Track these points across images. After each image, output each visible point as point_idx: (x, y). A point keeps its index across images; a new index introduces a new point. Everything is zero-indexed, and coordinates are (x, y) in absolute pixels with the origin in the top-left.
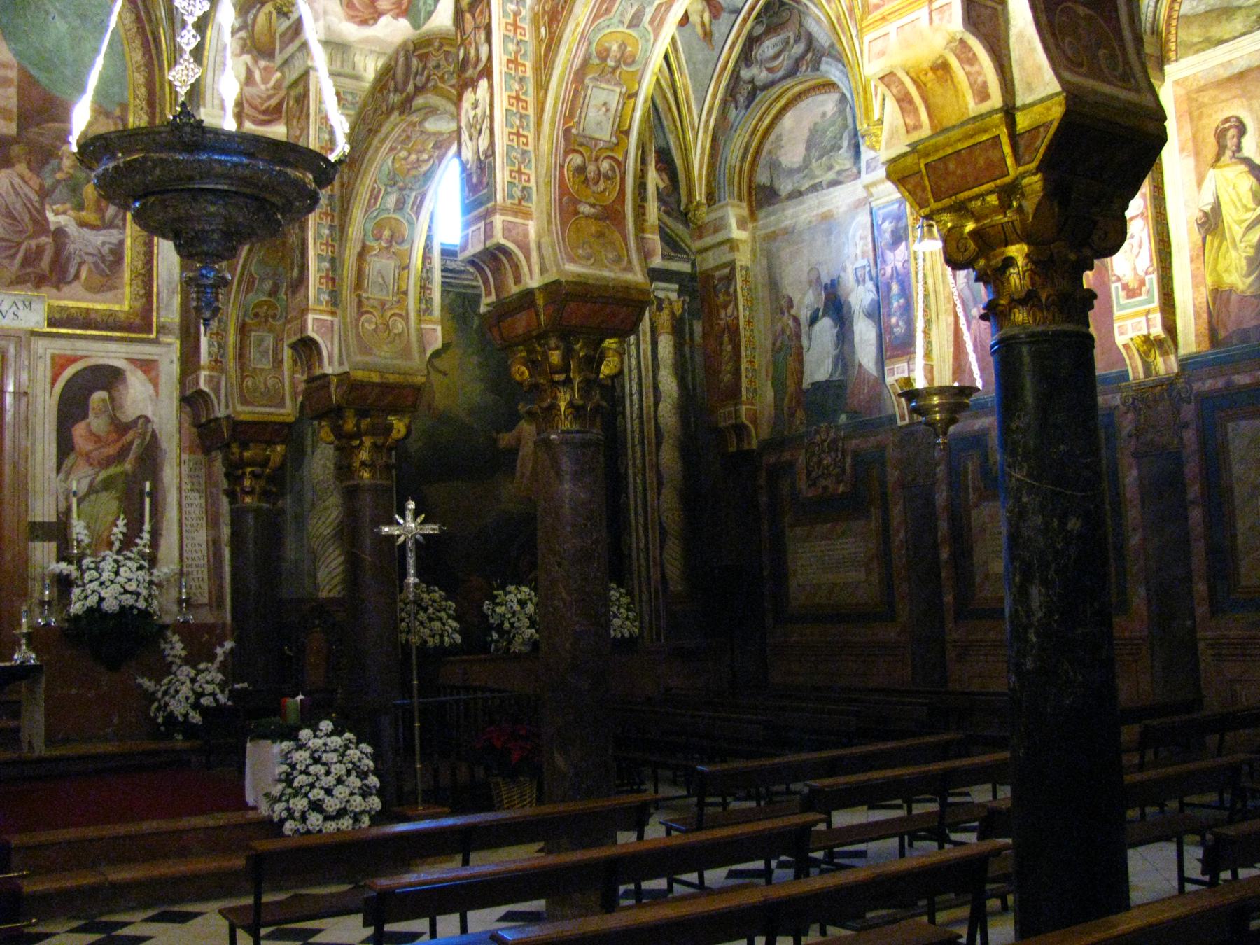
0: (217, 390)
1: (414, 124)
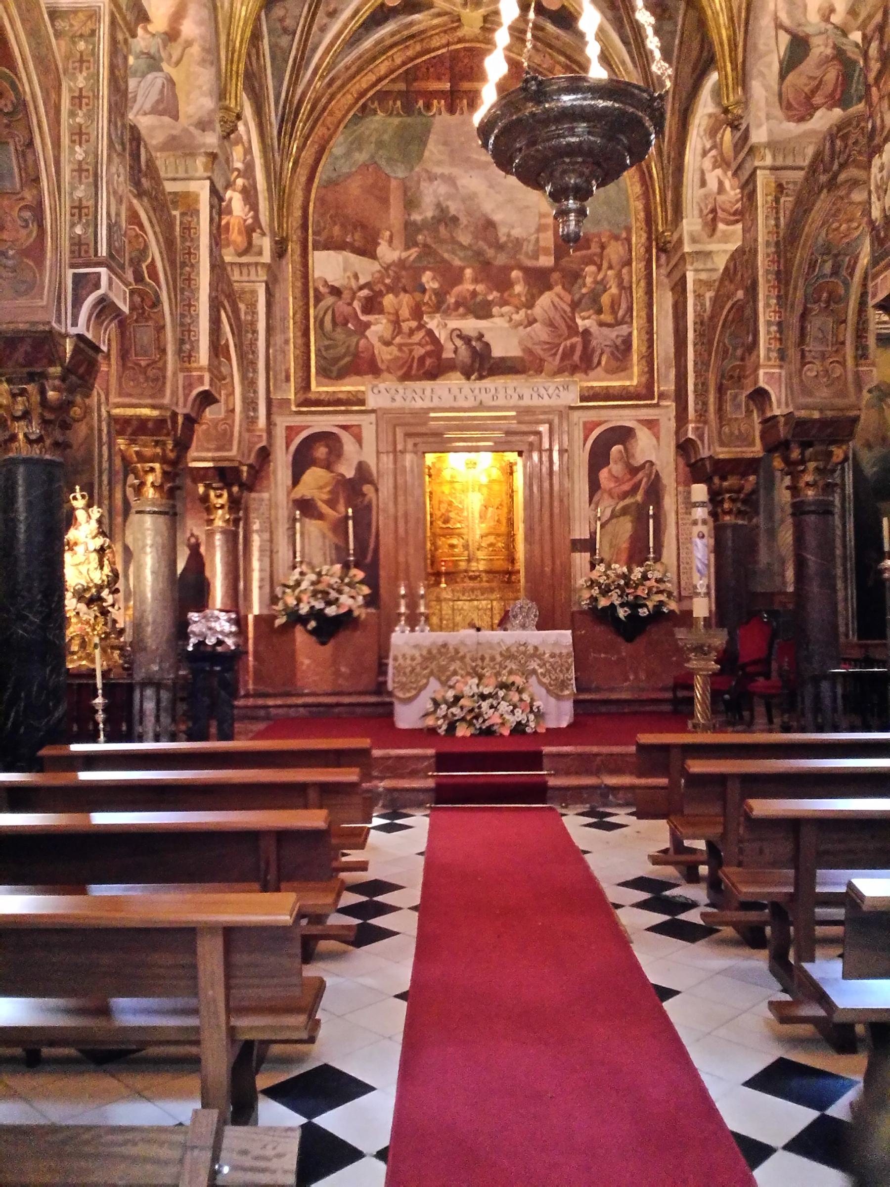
0: (701, 438)
1: (842, 198)
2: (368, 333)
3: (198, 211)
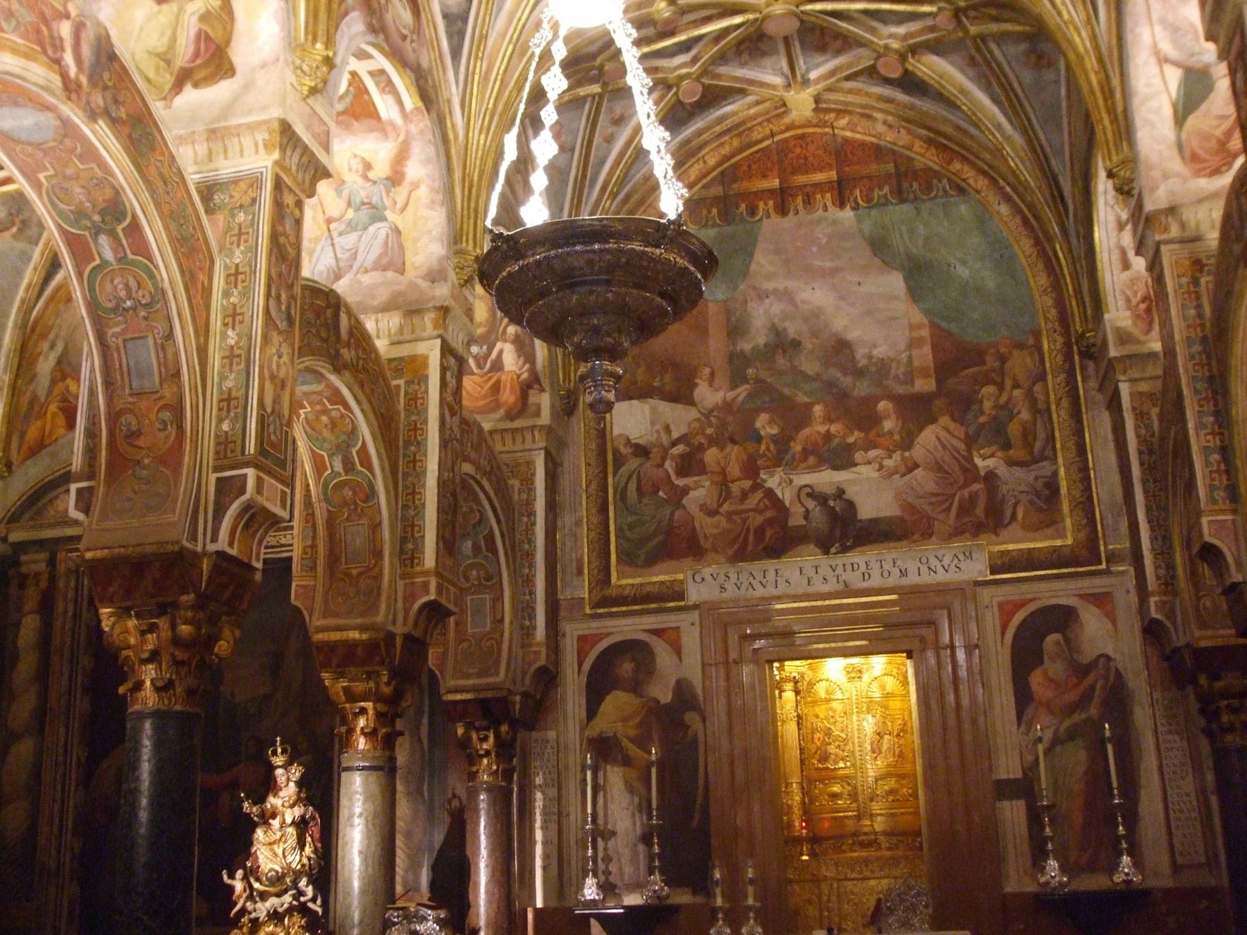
2: (684, 502)
3: (427, 377)
